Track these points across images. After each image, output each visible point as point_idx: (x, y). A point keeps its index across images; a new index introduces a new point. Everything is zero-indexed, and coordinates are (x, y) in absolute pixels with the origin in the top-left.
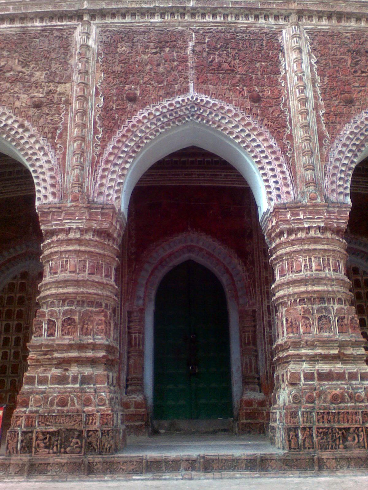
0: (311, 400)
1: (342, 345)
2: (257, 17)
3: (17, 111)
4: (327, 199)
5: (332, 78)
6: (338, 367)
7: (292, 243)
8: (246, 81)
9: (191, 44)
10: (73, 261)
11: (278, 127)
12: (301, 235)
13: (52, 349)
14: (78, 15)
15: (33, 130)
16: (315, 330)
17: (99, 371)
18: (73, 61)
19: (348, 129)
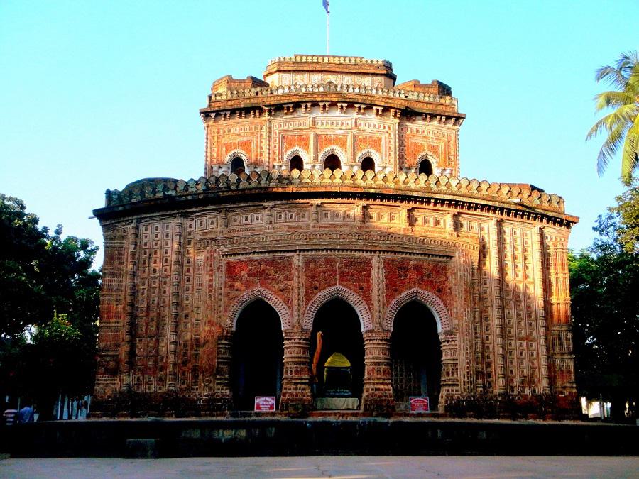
0: (372, 396)
1: (384, 380)
2: (363, 251)
3: (274, 293)
4: (383, 329)
5: (390, 280)
6: (382, 387)
7: (371, 344)
8: (358, 280)
9: (338, 264)
10: (297, 350)
11: (368, 300)
12: (374, 342)
13: (291, 379)
14: (295, 251)
15: (281, 301)
16: (375, 374)
17: (307, 386)
18: (294, 271)
19: (394, 301)
